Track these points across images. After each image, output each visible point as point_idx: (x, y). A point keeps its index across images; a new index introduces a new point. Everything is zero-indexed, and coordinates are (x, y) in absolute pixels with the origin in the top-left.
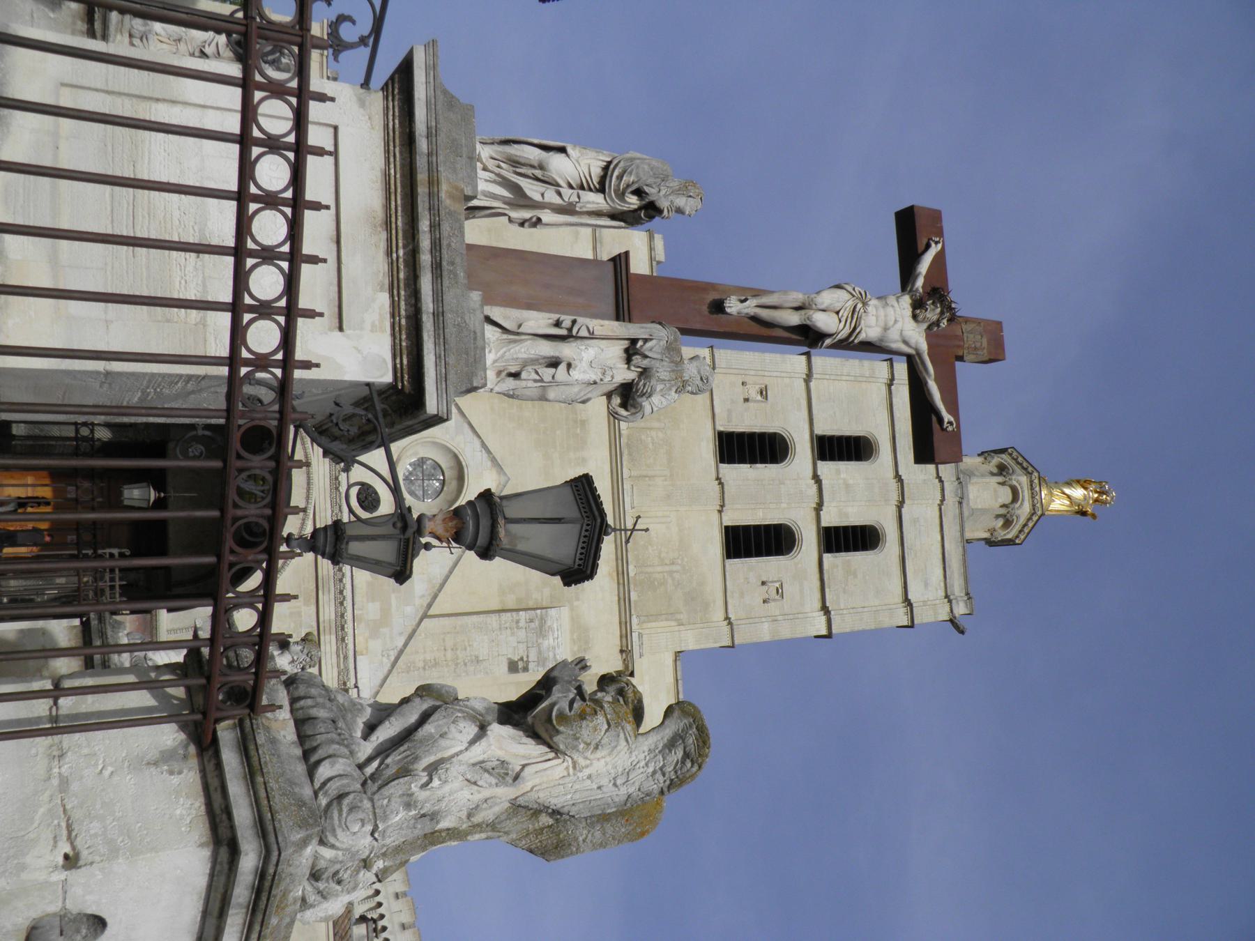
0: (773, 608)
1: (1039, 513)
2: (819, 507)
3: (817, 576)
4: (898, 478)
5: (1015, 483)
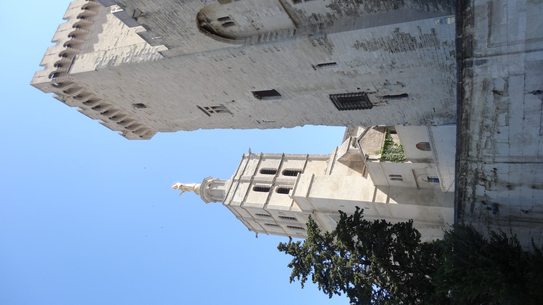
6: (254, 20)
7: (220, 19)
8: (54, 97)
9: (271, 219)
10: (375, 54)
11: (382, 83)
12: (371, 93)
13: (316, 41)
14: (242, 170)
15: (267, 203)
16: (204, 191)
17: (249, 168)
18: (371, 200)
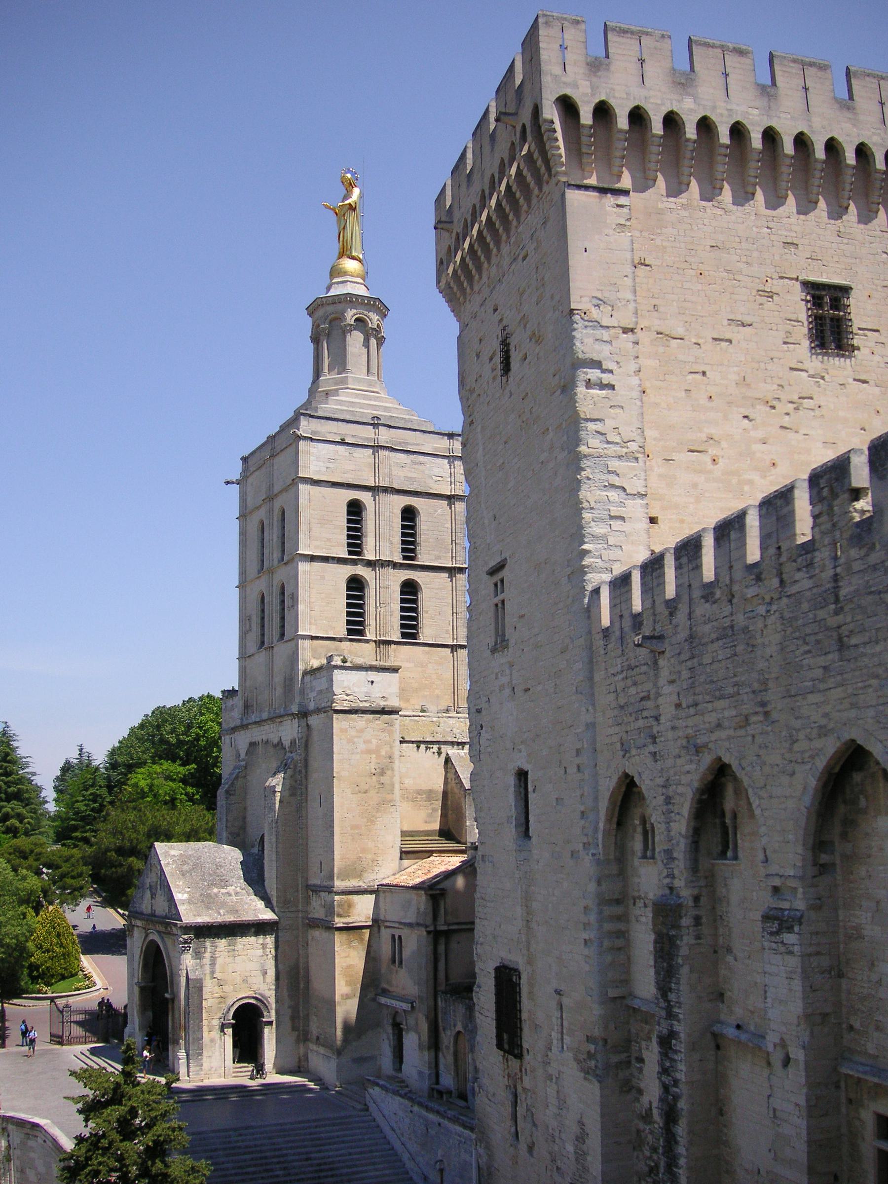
8: (513, 61)
9: (276, 555)
14: (407, 444)
15: (313, 558)
16: (339, 307)
17: (416, 466)
18: (339, 884)
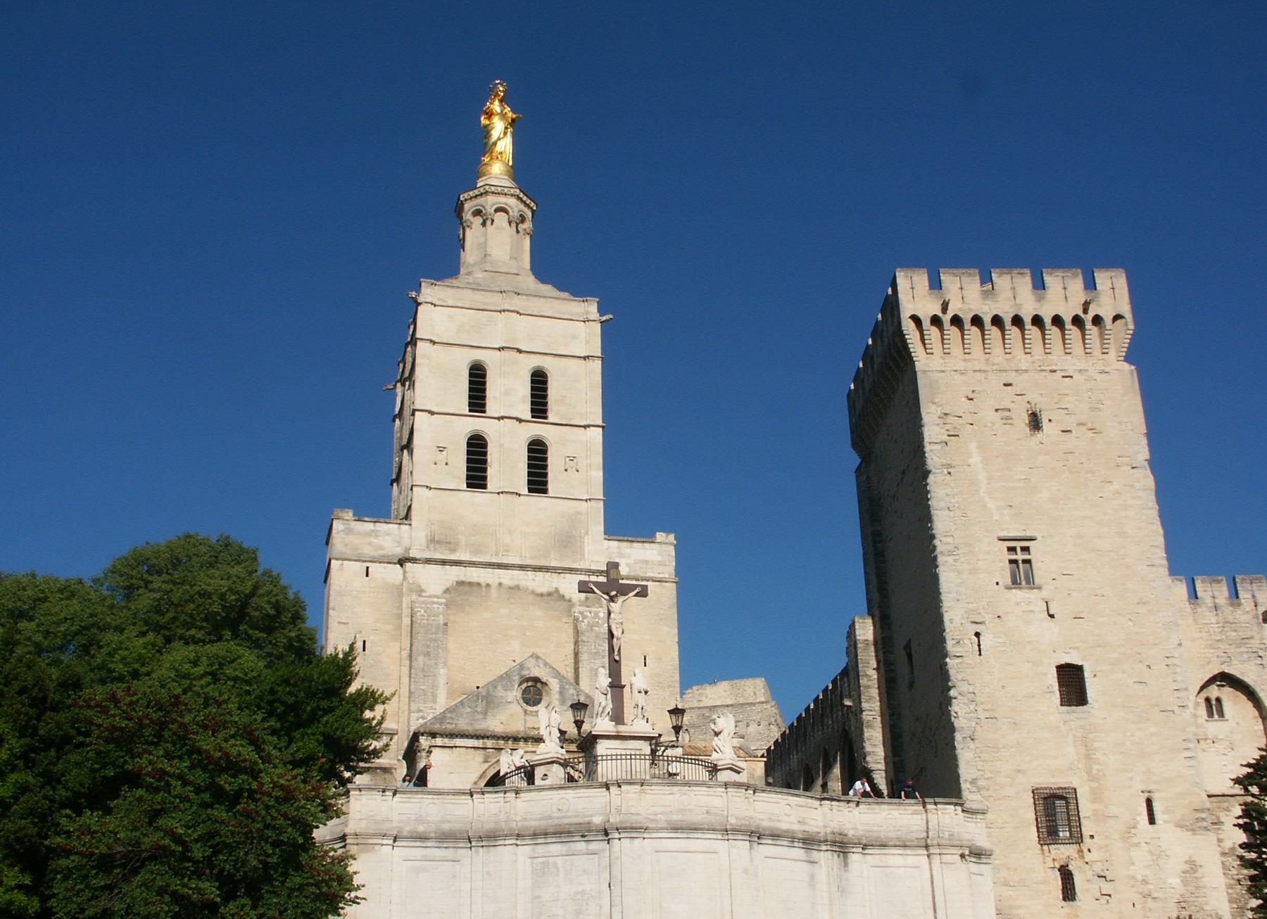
0: (582, 465)
1: (518, 191)
2: (520, 420)
3: (563, 427)
4: (499, 349)
5: (492, 211)
6: (1215, 744)
7: (1218, 700)
10: (1175, 881)
11: (1106, 873)
12: (1080, 851)
13: (1203, 815)
